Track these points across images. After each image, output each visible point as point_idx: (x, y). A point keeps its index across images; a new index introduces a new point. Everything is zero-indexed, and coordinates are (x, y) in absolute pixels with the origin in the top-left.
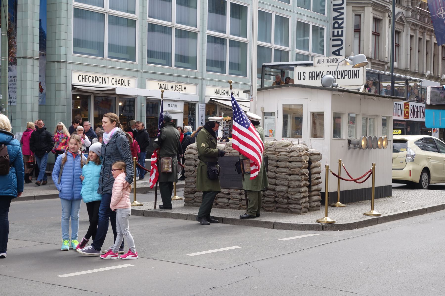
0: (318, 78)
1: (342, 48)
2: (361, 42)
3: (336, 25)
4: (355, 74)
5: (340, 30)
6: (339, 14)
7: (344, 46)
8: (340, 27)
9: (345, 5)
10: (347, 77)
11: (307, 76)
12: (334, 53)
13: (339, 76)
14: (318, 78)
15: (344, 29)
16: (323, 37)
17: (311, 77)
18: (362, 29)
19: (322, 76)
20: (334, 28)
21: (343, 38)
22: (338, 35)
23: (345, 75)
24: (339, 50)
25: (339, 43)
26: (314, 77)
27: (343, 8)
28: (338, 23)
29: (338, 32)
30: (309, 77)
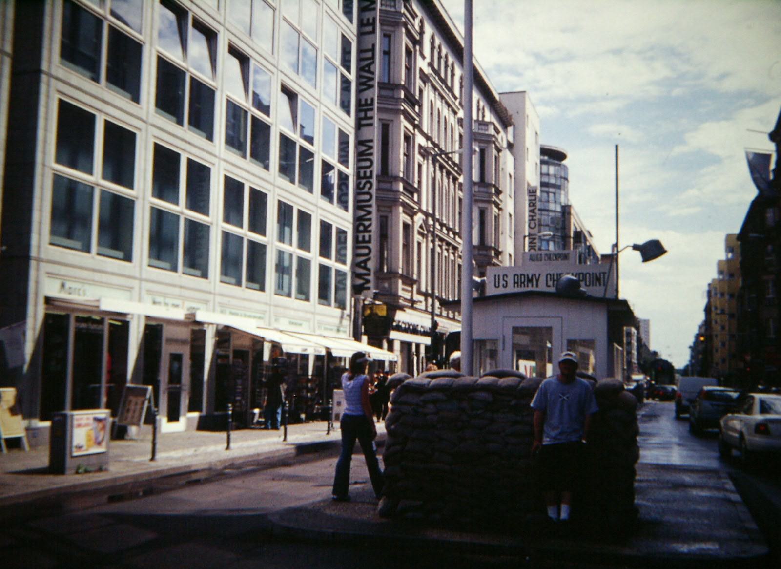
0: (530, 285)
1: (369, 259)
3: (361, 228)
4: (598, 279)
5: (367, 235)
6: (365, 213)
7: (372, 255)
8: (366, 230)
9: (373, 202)
11: (510, 280)
14: (530, 285)
15: (372, 234)
16: (345, 242)
17: (518, 283)
19: (537, 281)
21: (371, 245)
22: (364, 241)
24: (365, 262)
25: (366, 251)
26: (524, 283)
27: (370, 206)
28: (364, 225)
30: (515, 283)
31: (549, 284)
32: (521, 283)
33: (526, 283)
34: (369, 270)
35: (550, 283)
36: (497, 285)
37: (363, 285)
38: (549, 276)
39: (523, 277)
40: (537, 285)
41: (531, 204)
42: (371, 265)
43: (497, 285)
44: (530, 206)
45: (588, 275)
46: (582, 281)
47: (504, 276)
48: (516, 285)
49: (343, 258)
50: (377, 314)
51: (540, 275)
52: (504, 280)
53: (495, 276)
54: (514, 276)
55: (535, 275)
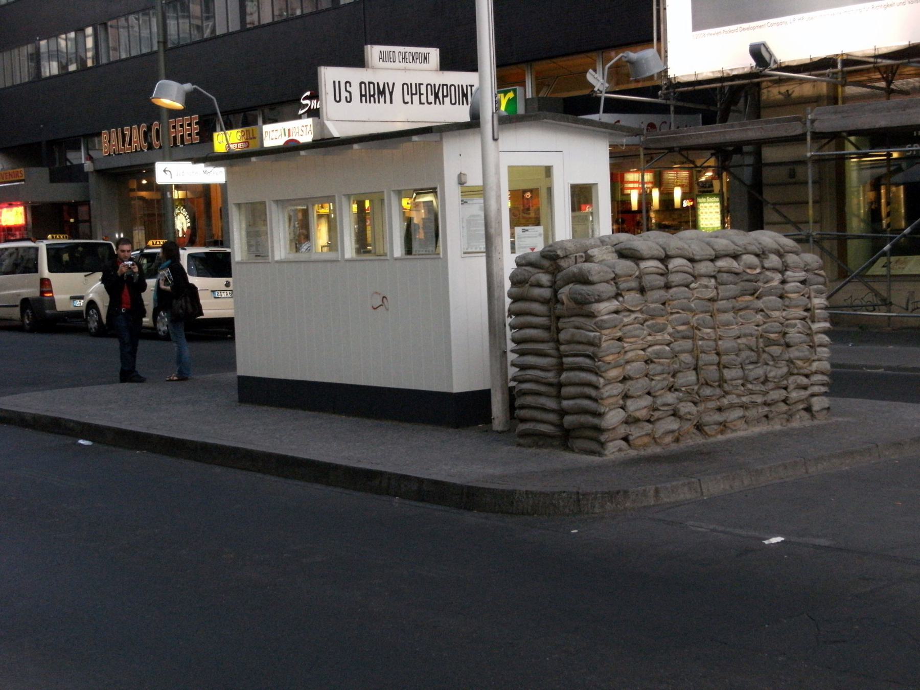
0: (382, 100)
4: (465, 95)
10: (447, 100)
11: (355, 90)
13: (431, 98)
14: (382, 100)
17: (365, 96)
19: (391, 94)
23: (444, 97)
26: (373, 96)
30: (362, 96)
32: (370, 96)
33: (376, 96)
35: (408, 98)
40: (391, 102)
46: (447, 96)
47: (346, 83)
48: (364, 98)
54: (361, 83)
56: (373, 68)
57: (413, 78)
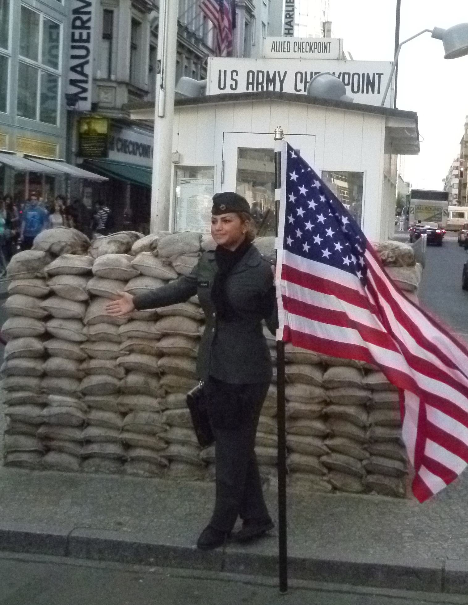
1: (87, 62)
2: (113, 55)
3: (78, 23)
4: (371, 84)
5: (85, 32)
7: (90, 58)
8: (84, 26)
12: (73, 69)
15: (92, 31)
16: (57, 40)
17: (253, 84)
18: (114, 35)
19: (282, 82)
20: (74, 27)
21: (90, 46)
22: (81, 40)
24: (82, 65)
25: (83, 52)
26: (262, 84)
29: (81, 34)
30: (248, 83)
31: (298, 88)
32: (258, 83)
33: (265, 84)
34: (86, 76)
35: (301, 86)
36: (222, 86)
37: (76, 95)
38: (299, 75)
39: (260, 74)
41: (288, 16)
42: (88, 69)
43: (222, 86)
44: (286, 17)
45: (356, 77)
46: (348, 84)
48: (250, 86)
49: (54, 60)
50: (95, 131)
51: (286, 73)
52: (232, 79)
53: (220, 71)
54: (248, 73)
55: (279, 72)
56: (264, 57)
57: (308, 67)
